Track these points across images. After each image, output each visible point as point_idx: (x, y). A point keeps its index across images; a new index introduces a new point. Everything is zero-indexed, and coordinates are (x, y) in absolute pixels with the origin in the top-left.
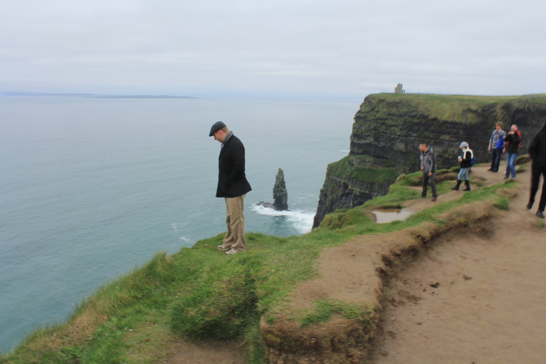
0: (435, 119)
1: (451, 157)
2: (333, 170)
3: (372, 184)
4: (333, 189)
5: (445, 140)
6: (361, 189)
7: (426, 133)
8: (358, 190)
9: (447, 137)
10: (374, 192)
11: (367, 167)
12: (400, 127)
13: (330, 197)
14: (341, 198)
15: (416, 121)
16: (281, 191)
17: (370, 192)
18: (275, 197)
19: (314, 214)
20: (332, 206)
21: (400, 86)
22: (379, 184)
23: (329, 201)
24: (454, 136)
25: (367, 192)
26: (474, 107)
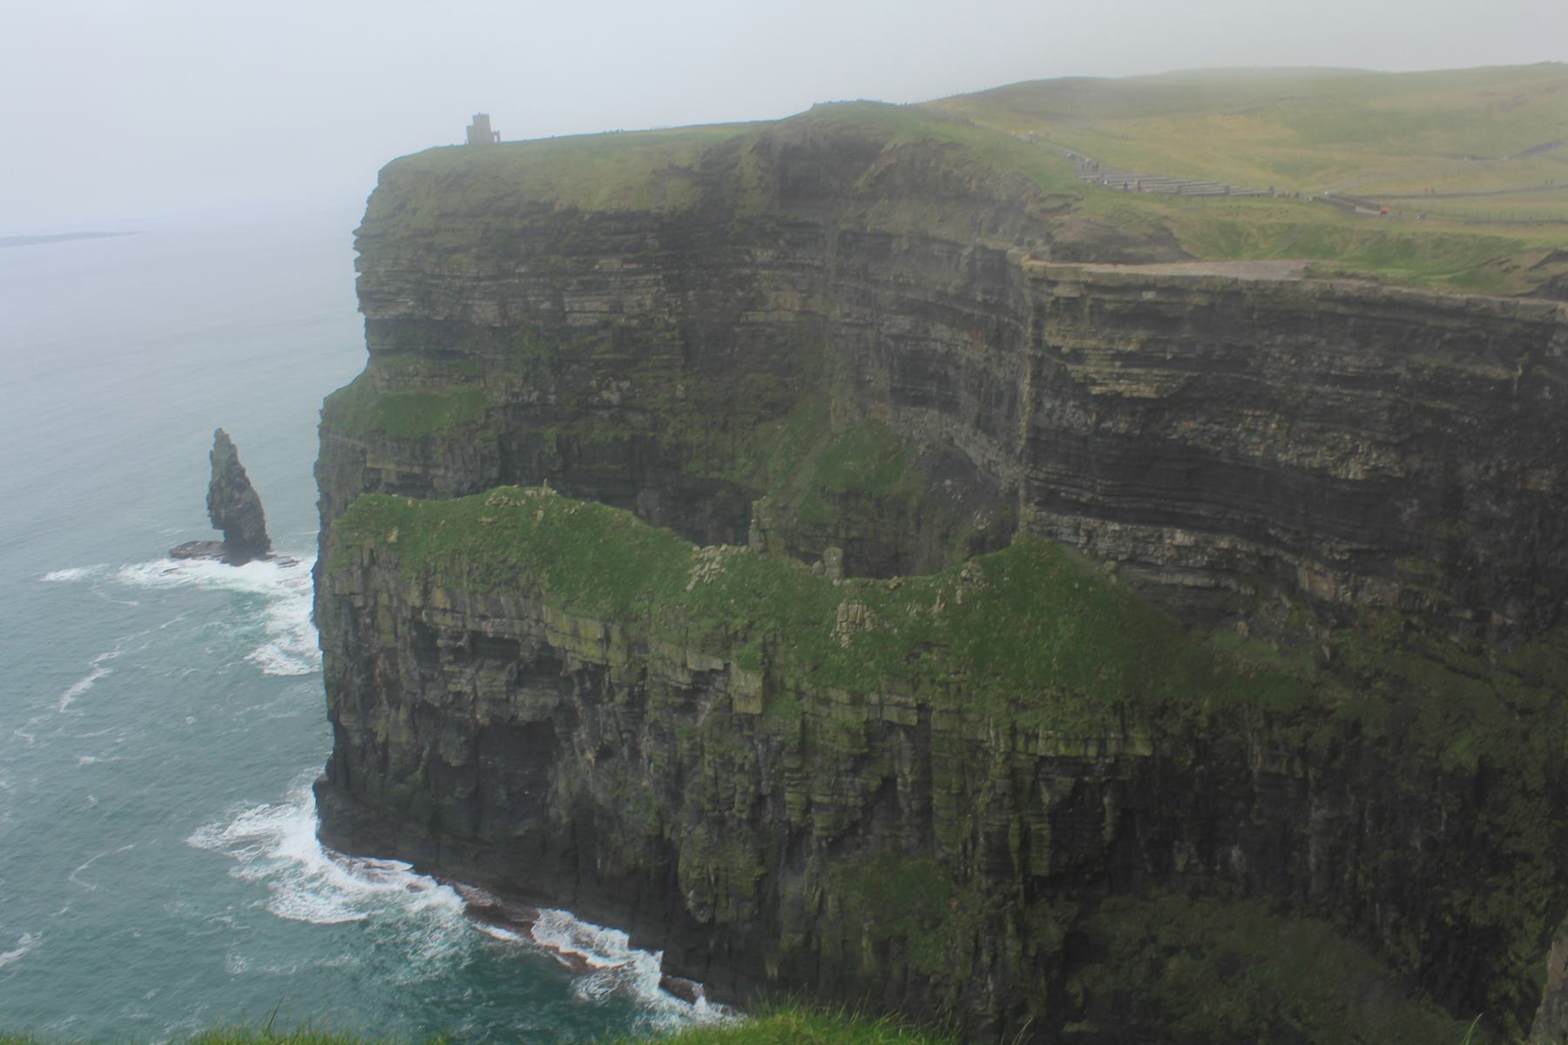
0: (572, 212)
1: (635, 322)
2: (336, 412)
5: (611, 274)
6: (398, 464)
7: (553, 259)
8: (392, 466)
9: (613, 263)
10: (438, 466)
12: (474, 250)
15: (517, 225)
18: (217, 522)
21: (481, 121)
24: (630, 256)
25: (417, 470)
26: (684, 159)
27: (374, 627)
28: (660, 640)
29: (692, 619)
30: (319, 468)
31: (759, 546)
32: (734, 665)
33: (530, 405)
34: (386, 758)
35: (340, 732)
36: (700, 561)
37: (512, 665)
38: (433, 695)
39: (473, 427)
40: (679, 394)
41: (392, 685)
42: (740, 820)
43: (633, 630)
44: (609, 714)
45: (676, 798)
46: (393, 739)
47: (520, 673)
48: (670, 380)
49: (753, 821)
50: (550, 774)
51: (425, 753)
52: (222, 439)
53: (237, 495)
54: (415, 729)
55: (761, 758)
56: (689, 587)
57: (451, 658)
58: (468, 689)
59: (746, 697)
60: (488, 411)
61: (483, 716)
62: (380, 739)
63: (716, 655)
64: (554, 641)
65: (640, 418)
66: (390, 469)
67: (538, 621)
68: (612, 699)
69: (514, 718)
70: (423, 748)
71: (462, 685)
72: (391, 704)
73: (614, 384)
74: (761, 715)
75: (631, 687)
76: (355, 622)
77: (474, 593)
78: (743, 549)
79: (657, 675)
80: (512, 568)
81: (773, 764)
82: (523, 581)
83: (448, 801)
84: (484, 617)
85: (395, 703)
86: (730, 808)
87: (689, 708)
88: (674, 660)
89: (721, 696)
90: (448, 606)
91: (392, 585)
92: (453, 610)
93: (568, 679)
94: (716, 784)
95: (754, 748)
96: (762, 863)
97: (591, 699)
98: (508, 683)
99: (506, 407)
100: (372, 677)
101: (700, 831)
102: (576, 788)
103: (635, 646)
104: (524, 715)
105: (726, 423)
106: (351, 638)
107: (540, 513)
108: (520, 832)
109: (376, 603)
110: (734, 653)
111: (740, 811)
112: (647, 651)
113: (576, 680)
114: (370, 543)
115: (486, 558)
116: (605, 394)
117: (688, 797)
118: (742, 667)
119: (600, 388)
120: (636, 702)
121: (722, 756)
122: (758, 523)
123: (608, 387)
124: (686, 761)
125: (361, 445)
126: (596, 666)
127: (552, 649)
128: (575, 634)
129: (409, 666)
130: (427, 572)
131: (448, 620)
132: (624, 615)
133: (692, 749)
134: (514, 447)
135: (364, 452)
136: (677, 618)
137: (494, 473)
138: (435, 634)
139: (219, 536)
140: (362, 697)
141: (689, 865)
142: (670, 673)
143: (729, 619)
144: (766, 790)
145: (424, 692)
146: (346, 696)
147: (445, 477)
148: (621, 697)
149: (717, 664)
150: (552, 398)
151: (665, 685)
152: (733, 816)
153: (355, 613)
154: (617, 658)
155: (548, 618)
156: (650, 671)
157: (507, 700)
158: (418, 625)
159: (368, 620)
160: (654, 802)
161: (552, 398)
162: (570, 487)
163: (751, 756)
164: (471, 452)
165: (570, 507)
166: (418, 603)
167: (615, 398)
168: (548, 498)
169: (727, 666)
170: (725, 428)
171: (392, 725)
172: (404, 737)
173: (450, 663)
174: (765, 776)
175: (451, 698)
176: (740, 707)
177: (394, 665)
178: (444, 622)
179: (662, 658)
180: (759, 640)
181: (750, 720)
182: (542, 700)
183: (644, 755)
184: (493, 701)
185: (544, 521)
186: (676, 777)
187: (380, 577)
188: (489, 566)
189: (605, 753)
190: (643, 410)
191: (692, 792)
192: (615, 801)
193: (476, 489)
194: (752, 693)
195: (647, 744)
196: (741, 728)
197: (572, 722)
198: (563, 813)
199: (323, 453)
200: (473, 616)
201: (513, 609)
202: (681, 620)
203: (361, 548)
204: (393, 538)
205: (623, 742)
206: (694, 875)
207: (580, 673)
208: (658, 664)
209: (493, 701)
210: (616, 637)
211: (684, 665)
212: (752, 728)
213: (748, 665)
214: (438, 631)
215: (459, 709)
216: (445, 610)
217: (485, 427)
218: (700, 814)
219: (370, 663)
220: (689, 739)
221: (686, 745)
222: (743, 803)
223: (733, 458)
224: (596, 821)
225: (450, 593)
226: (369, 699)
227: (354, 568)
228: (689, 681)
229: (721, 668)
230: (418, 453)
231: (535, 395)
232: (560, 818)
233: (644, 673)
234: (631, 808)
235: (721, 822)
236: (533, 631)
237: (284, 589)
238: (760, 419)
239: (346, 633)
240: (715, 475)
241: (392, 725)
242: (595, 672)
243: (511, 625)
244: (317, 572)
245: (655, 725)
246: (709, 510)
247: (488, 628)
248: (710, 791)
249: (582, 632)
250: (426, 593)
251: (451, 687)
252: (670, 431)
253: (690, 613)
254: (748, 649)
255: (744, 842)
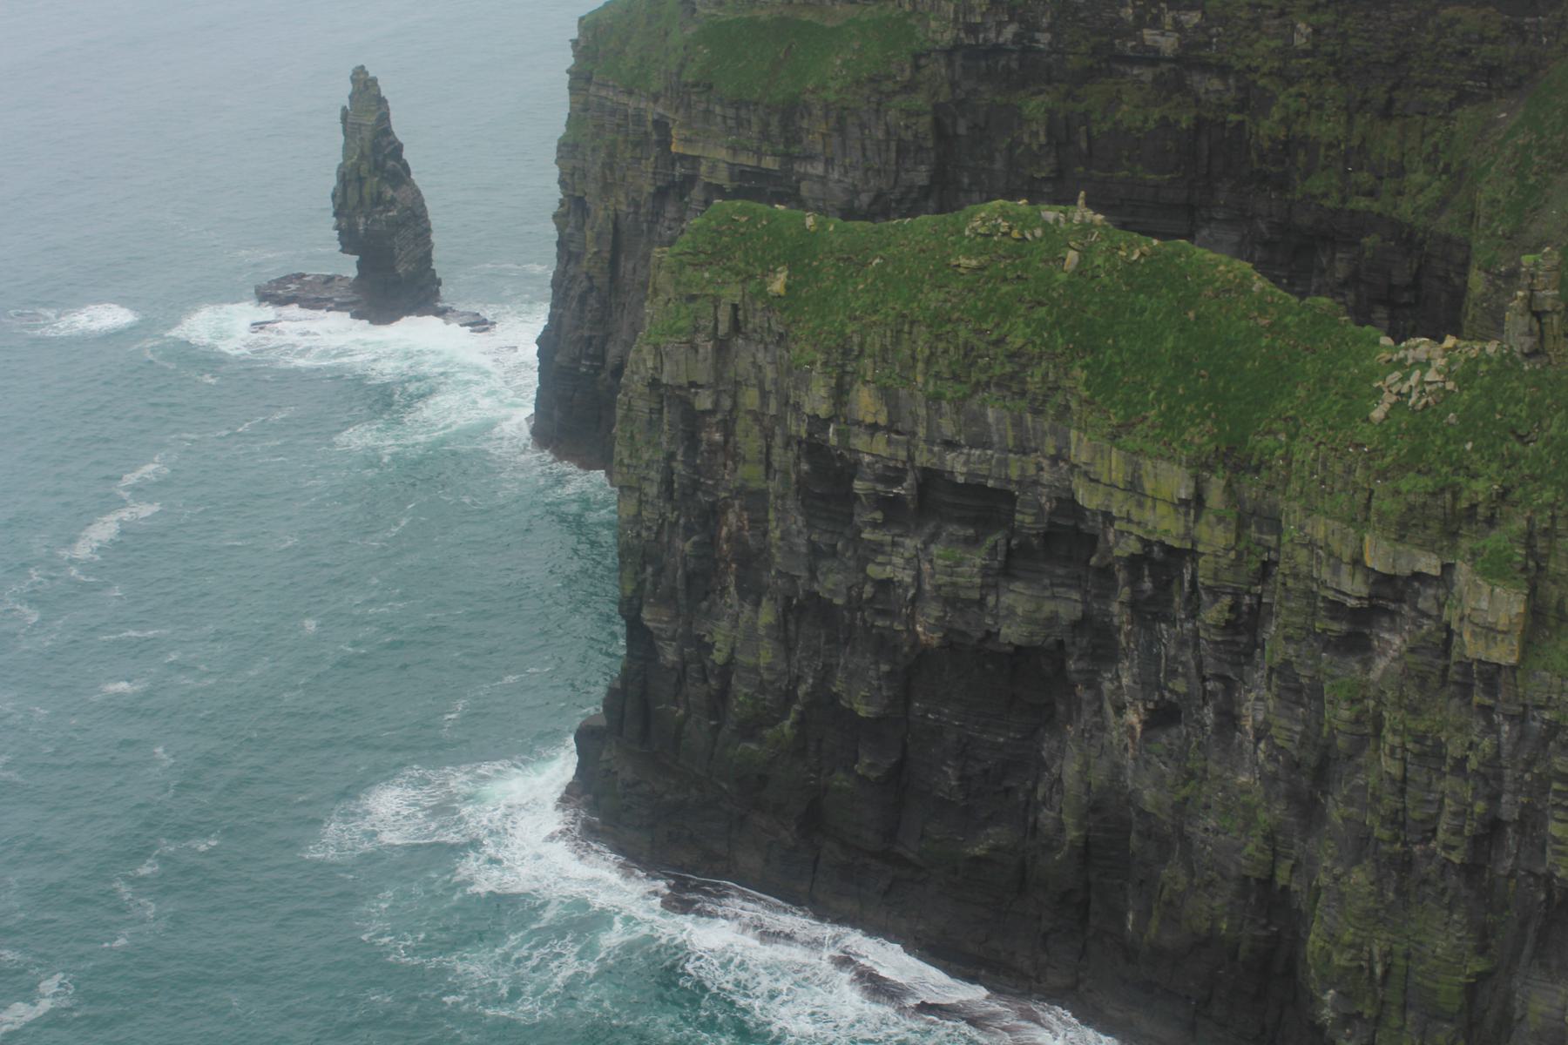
3: (791, 111)
4: (609, 165)
6: (734, 149)
8: (723, 154)
10: (810, 158)
11: (763, 15)
13: (600, 214)
14: (656, 215)
16: (378, 199)
17: (788, 158)
18: (350, 241)
19: (538, 320)
20: (614, 263)
22: (827, 106)
23: (599, 236)
25: (770, 163)
27: (728, 450)
28: (1310, 510)
29: (1383, 474)
30: (568, 150)
31: (1528, 343)
32: (1463, 571)
33: (998, 50)
34: (724, 693)
35: (638, 634)
36: (1400, 364)
37: (998, 537)
38: (832, 584)
39: (888, 86)
40: (1300, 41)
41: (750, 560)
42: (1446, 864)
43: (1251, 489)
44: (1182, 644)
45: (1309, 810)
46: (740, 657)
47: (1009, 553)
48: (1282, 14)
49: (1471, 870)
50: (1049, 745)
51: (802, 690)
52: (365, 89)
53: (389, 193)
54: (787, 645)
55: (1507, 749)
56: (1377, 414)
57: (878, 516)
58: (907, 577)
59: (1490, 632)
60: (917, 57)
61: (930, 629)
62: (719, 657)
63: (1429, 546)
64: (1088, 498)
65: (1216, 84)
66: (716, 158)
67: (1055, 460)
68: (1193, 615)
69: (990, 635)
70: (799, 679)
71: (895, 568)
72: (743, 594)
73: (1168, 19)
74: (1513, 668)
75: (1237, 594)
76: (692, 440)
77: (937, 397)
78: (1491, 348)
79: (1296, 576)
80: (1012, 356)
81: (1529, 764)
82: (1034, 379)
83: (840, 780)
84: (950, 445)
85: (752, 592)
86: (1426, 841)
87: (1356, 644)
88: (1336, 545)
89: (1428, 625)
90: (882, 420)
91: (770, 373)
92: (890, 428)
93: (1106, 572)
94: (1402, 792)
95: (1492, 728)
96: (1482, 951)
97: (1149, 611)
98: (985, 571)
99: (950, 52)
100: (713, 541)
101: (1359, 877)
102: (1099, 776)
103: (1254, 518)
104: (1012, 633)
105: (1390, 102)
106: (679, 467)
107: (1072, 256)
108: (979, 850)
109: (735, 405)
110: (1465, 544)
111: (1448, 847)
112: (1278, 529)
113: (1122, 576)
114: (732, 293)
115: (963, 333)
116: (1149, 35)
117: (1336, 813)
118: (1485, 573)
119: (1140, 23)
120: (1245, 625)
121: (1420, 739)
122: (1530, 300)
123: (1156, 23)
124: (1341, 742)
125: (653, 111)
126: (1169, 550)
127: (1076, 510)
128: (1133, 487)
129: (788, 529)
130: (846, 353)
131: (880, 445)
132: (1234, 458)
133: (1357, 721)
134: (962, 129)
135: (661, 125)
136: (1350, 471)
137: (921, 176)
138: (852, 469)
139: (348, 267)
140: (689, 578)
141: (1329, 939)
142: (1326, 574)
143: (1461, 479)
144: (1509, 809)
145: (813, 577)
146: (659, 573)
147: (823, 180)
148: (1214, 613)
149: (1429, 564)
150: (1044, 39)
151: (1310, 595)
152: (1431, 855)
153: (692, 422)
154: (1214, 538)
155: (1080, 452)
156: (1284, 567)
157: (981, 602)
158: (813, 449)
159: (718, 437)
160: (1262, 816)
161: (1044, 39)
162: (1129, 212)
163: (1486, 744)
164: (880, 135)
165: (1131, 246)
166: (823, 410)
167: (1168, 43)
168: (1086, 228)
169: (1447, 568)
170: (1386, 113)
171: (743, 631)
172: (766, 655)
173: (875, 525)
174: (1509, 785)
175: (868, 590)
176: (1472, 647)
177: (759, 523)
178: (871, 449)
179: (1310, 545)
180: (1519, 524)
181: (1492, 674)
182: (1049, 607)
183: (1248, 725)
184: (951, 601)
185: (1080, 271)
186: (1311, 776)
187: (745, 356)
188: (968, 349)
189: (1163, 716)
190: (1223, 70)
191: (1349, 801)
192: (1180, 807)
193: (880, 209)
194: (1503, 623)
195: (1256, 705)
196: (1466, 689)
197: (1104, 650)
198: (1069, 820)
199: (574, 121)
200: (930, 441)
201: (1010, 433)
202: (1359, 475)
203: (716, 301)
204: (777, 285)
205: (1206, 696)
206: (1340, 960)
207: (1134, 562)
208: (1302, 555)
209: (951, 601)
210: (1215, 497)
211: (1357, 562)
212: (1491, 688)
213: (1494, 569)
214: (858, 463)
215: (883, 613)
216: (874, 428)
217: (910, 87)
218: (1362, 844)
219: (713, 514)
220: (1353, 701)
221: (1345, 713)
222: (1458, 832)
223: (1400, 171)
224: (1134, 841)
225: (887, 394)
226: (701, 583)
227: (700, 339)
228: (1364, 591)
229: (1436, 572)
230: (775, 129)
231: (1009, 31)
232: (1061, 828)
233: (1266, 569)
234: (1211, 823)
235: (1405, 864)
236: (1046, 477)
237: (481, 364)
238: (1462, 97)
239: (671, 456)
240: (1362, 203)
241: (743, 631)
242: (1163, 563)
243: (1003, 463)
244: (548, 344)
245: (1283, 670)
246: (1341, 271)
247: (956, 465)
248: (1390, 802)
249: (1148, 486)
250: (840, 393)
251: (872, 570)
252: (1276, 113)
253: (1377, 464)
254: (1496, 539)
255: (1450, 908)
